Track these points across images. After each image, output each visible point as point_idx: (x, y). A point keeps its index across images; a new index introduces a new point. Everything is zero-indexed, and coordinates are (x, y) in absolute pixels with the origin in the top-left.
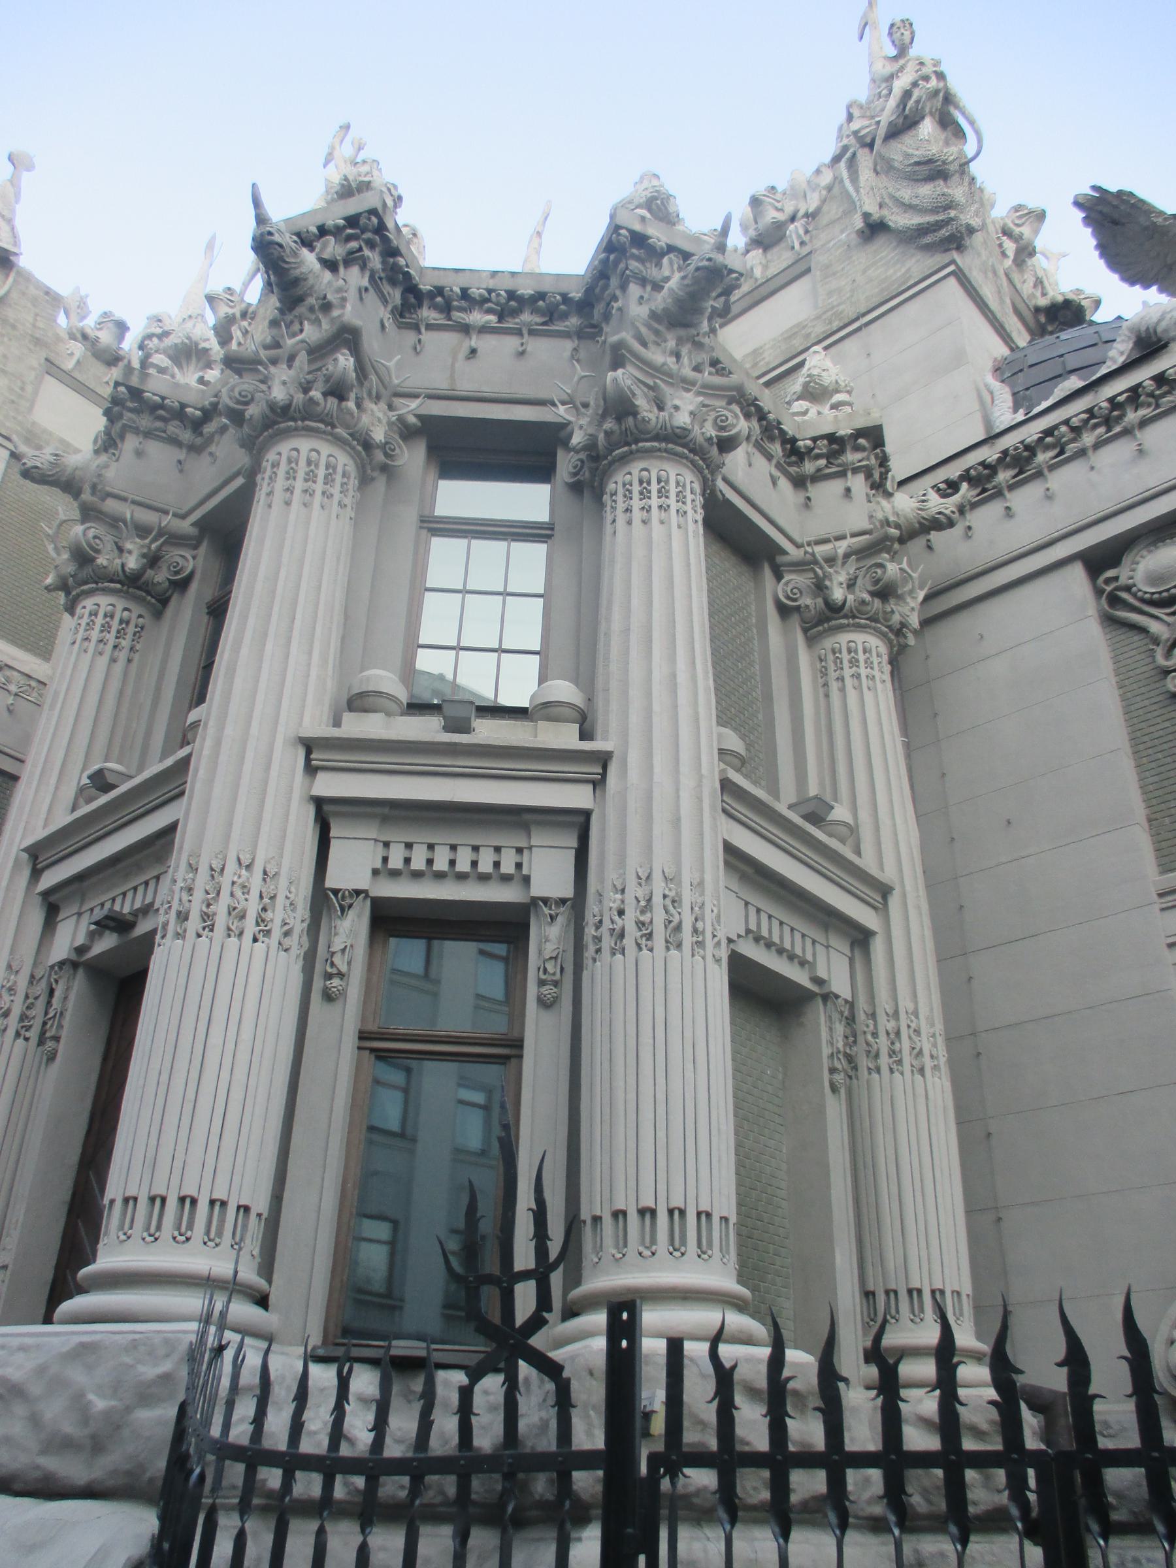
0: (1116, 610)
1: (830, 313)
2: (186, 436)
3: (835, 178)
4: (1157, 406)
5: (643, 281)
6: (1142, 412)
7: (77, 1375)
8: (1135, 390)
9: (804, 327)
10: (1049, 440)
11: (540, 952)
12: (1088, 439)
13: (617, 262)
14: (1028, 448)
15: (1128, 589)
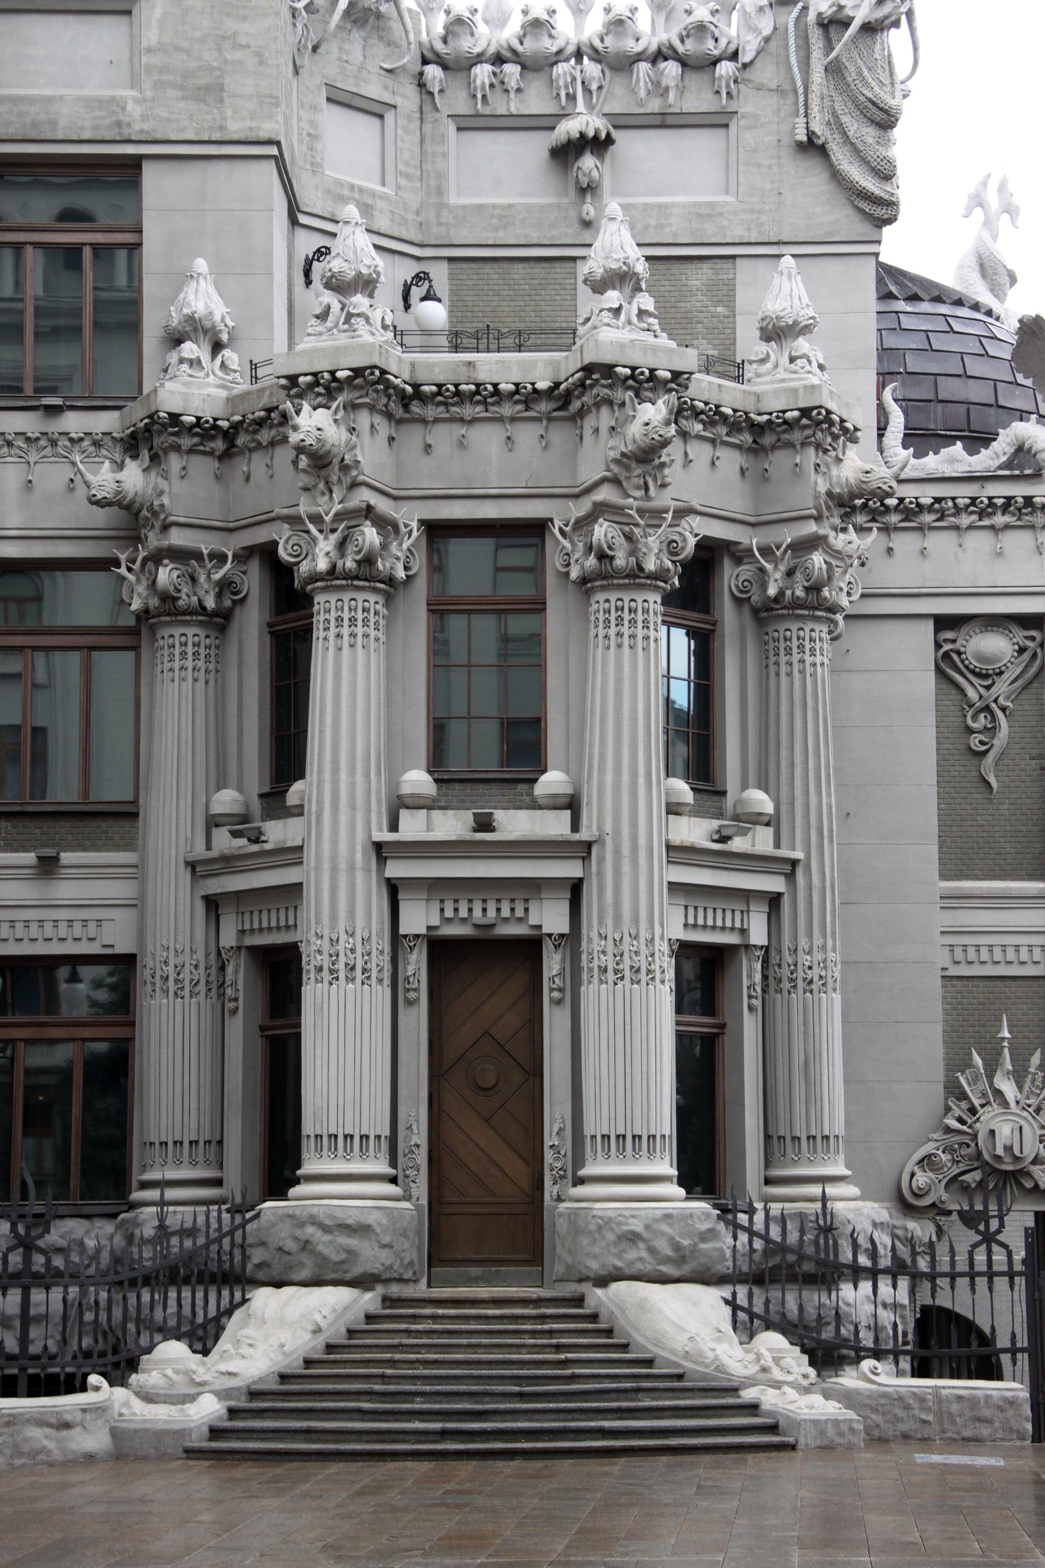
0: (948, 666)
1: (750, 216)
2: (399, 412)
3: (775, 29)
4: (1019, 519)
5: (818, 446)
6: (1007, 519)
7: (664, 1227)
8: (1009, 499)
9: (720, 214)
10: (937, 506)
11: (750, 977)
12: (965, 520)
13: (805, 427)
14: (918, 505)
15: (959, 653)
